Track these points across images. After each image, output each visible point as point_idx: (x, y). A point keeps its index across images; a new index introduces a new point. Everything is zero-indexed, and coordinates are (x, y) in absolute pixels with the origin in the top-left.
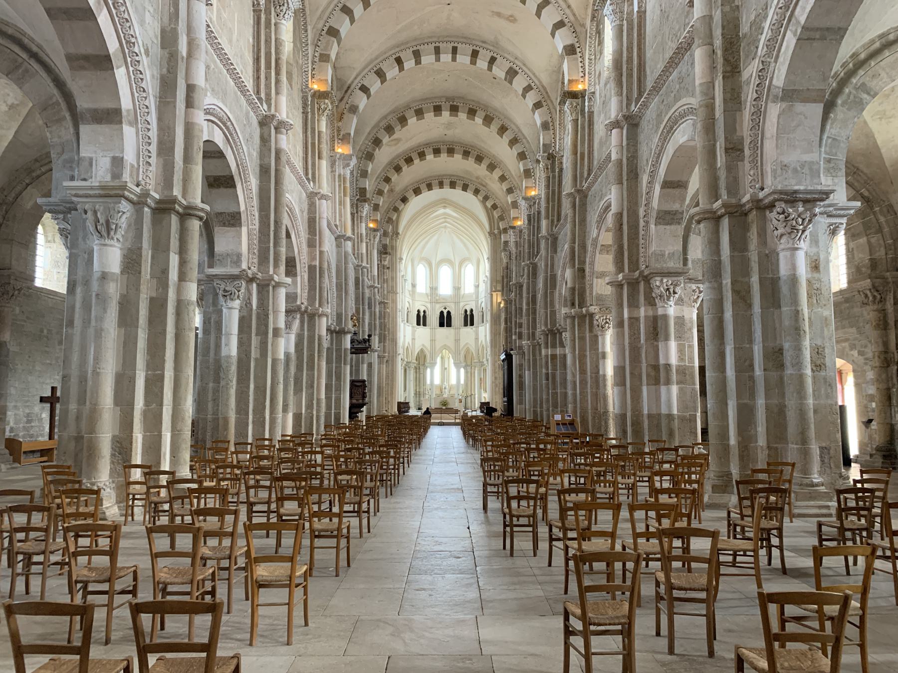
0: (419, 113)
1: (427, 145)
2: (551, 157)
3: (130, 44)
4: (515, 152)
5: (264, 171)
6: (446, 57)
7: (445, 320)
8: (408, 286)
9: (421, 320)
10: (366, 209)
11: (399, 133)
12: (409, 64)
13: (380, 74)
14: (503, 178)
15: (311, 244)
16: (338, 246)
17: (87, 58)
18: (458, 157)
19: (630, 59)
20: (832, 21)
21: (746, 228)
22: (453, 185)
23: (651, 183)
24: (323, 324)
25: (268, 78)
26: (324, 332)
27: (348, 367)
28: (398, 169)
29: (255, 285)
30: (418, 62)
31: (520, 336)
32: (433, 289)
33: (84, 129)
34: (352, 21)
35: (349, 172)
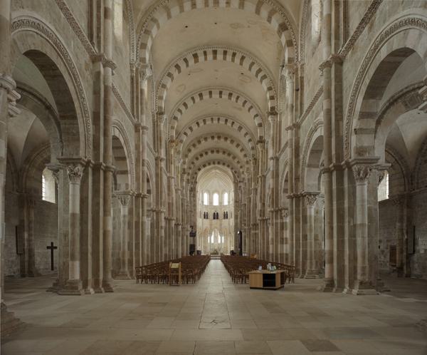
0: (206, 139)
1: (209, 149)
2: (255, 159)
3: (130, 152)
4: (243, 153)
5: (157, 175)
6: (216, 122)
7: (216, 216)
8: (200, 202)
9: (206, 216)
10: (185, 176)
11: (198, 146)
12: (202, 124)
13: (191, 129)
14: (238, 162)
15: (169, 195)
16: (176, 192)
17: (120, 158)
18: (221, 154)
19: (276, 138)
20: (319, 148)
21: (299, 200)
22: (219, 163)
23: (282, 179)
24: (174, 222)
25: (158, 144)
26: (173, 226)
27: (180, 238)
28: (197, 159)
29: (155, 213)
30: (205, 123)
31: (245, 225)
32: (211, 201)
33: (118, 177)
34: (181, 113)
35: (180, 164)
